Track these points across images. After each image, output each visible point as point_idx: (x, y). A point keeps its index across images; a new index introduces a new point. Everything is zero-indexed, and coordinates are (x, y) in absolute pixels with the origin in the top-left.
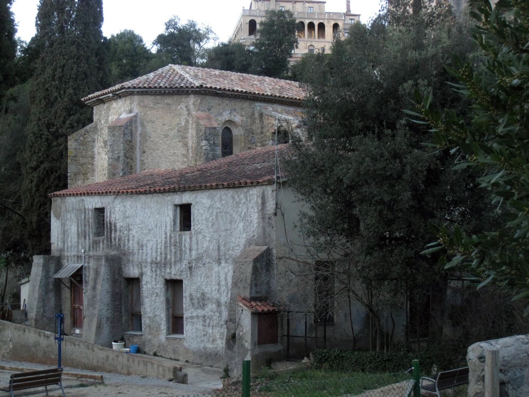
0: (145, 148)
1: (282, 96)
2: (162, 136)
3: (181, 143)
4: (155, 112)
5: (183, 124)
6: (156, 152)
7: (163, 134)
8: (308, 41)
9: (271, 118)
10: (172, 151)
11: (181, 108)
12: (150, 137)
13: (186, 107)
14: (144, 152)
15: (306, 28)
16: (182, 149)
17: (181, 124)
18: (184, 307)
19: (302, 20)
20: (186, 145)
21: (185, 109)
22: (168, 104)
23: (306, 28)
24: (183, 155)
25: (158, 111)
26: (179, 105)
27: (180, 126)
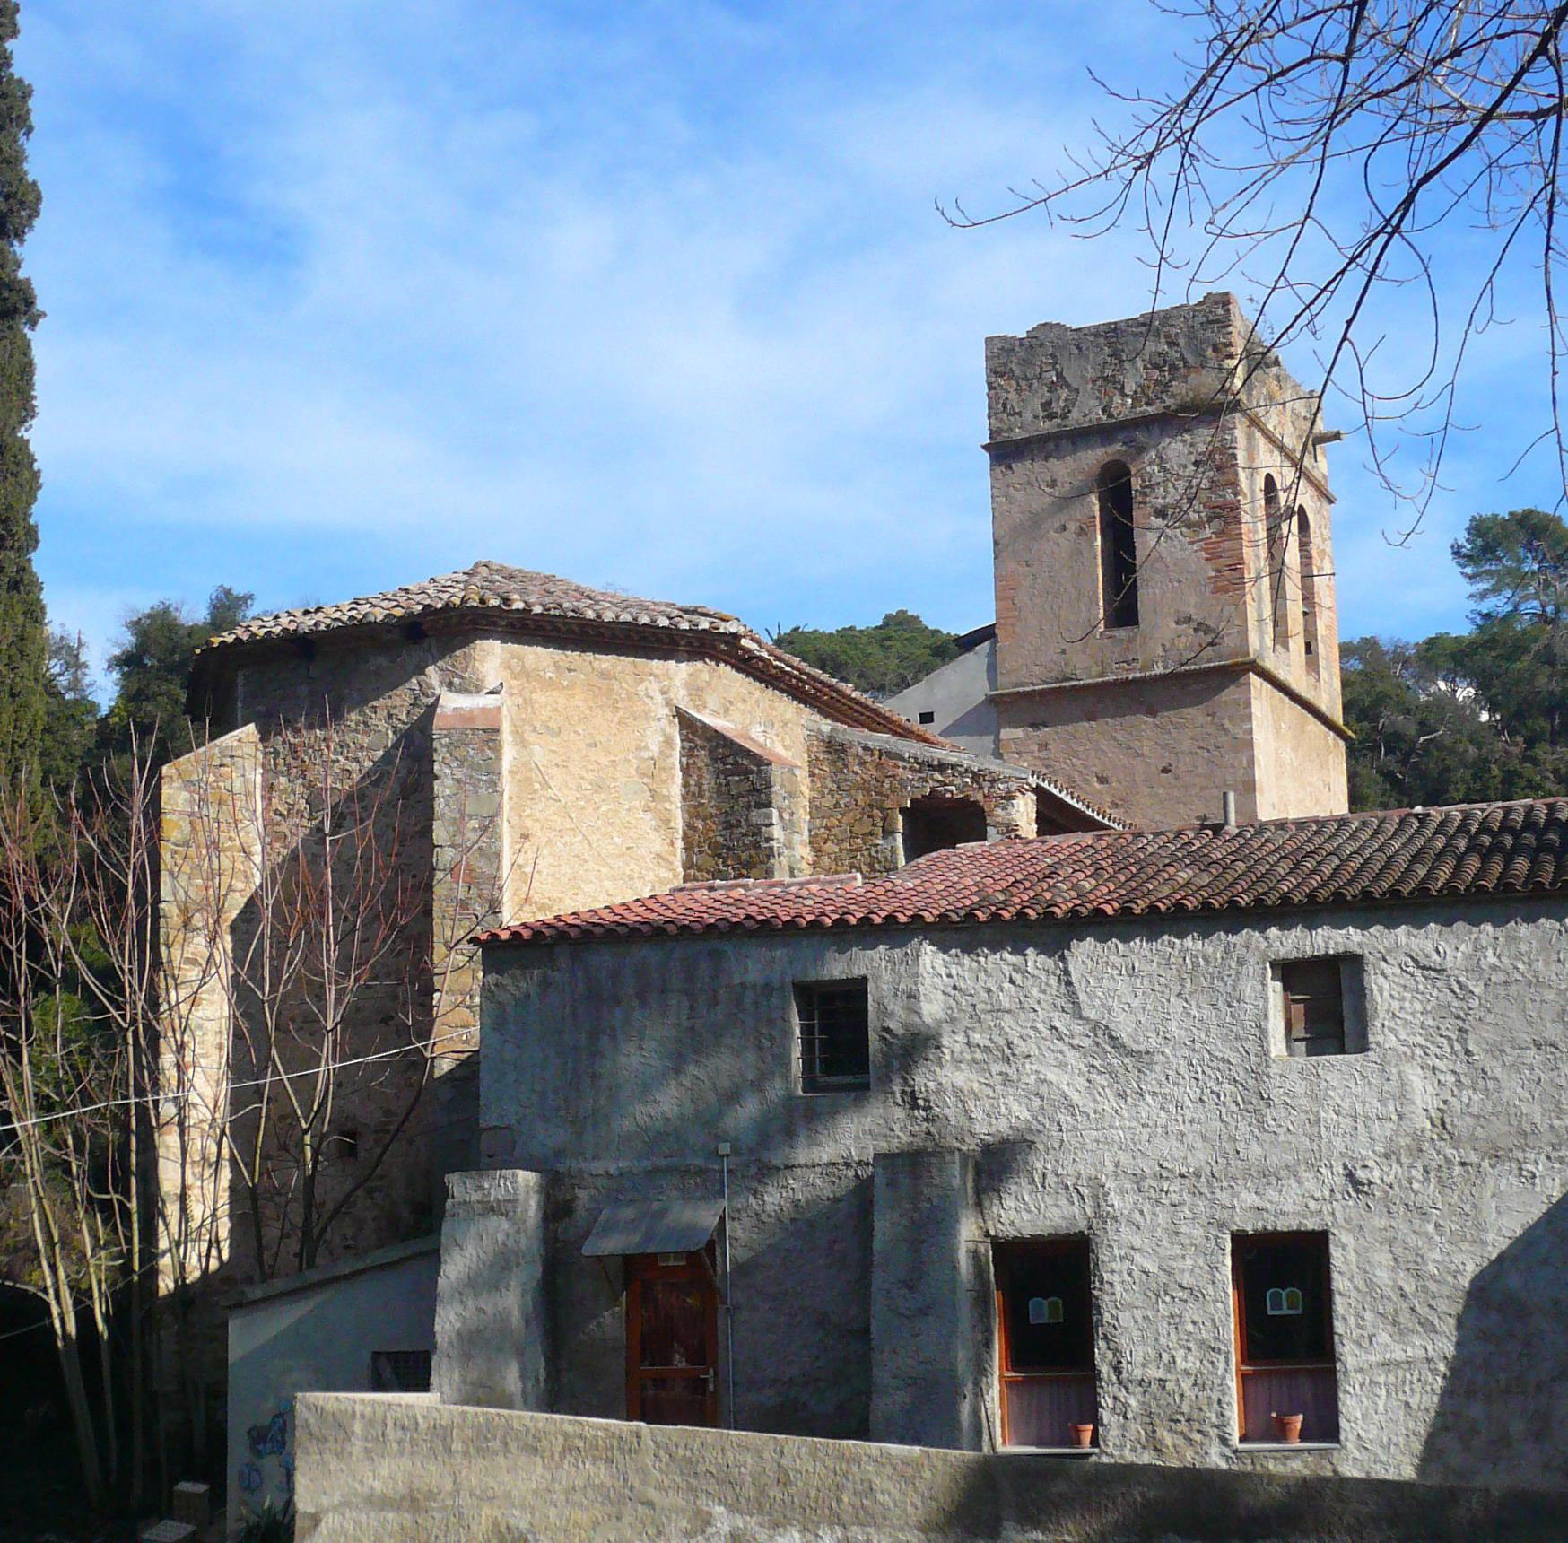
0: (529, 822)
2: (585, 785)
3: (649, 816)
4: (562, 701)
5: (655, 750)
6: (567, 839)
7: (590, 776)
9: (891, 763)
10: (618, 841)
11: (647, 695)
12: (546, 785)
13: (663, 693)
14: (525, 837)
16: (653, 835)
17: (646, 748)
18: (1339, 1326)
20: (669, 821)
21: (659, 698)
22: (604, 675)
24: (658, 856)
25: (573, 696)
26: (642, 681)
27: (645, 754)
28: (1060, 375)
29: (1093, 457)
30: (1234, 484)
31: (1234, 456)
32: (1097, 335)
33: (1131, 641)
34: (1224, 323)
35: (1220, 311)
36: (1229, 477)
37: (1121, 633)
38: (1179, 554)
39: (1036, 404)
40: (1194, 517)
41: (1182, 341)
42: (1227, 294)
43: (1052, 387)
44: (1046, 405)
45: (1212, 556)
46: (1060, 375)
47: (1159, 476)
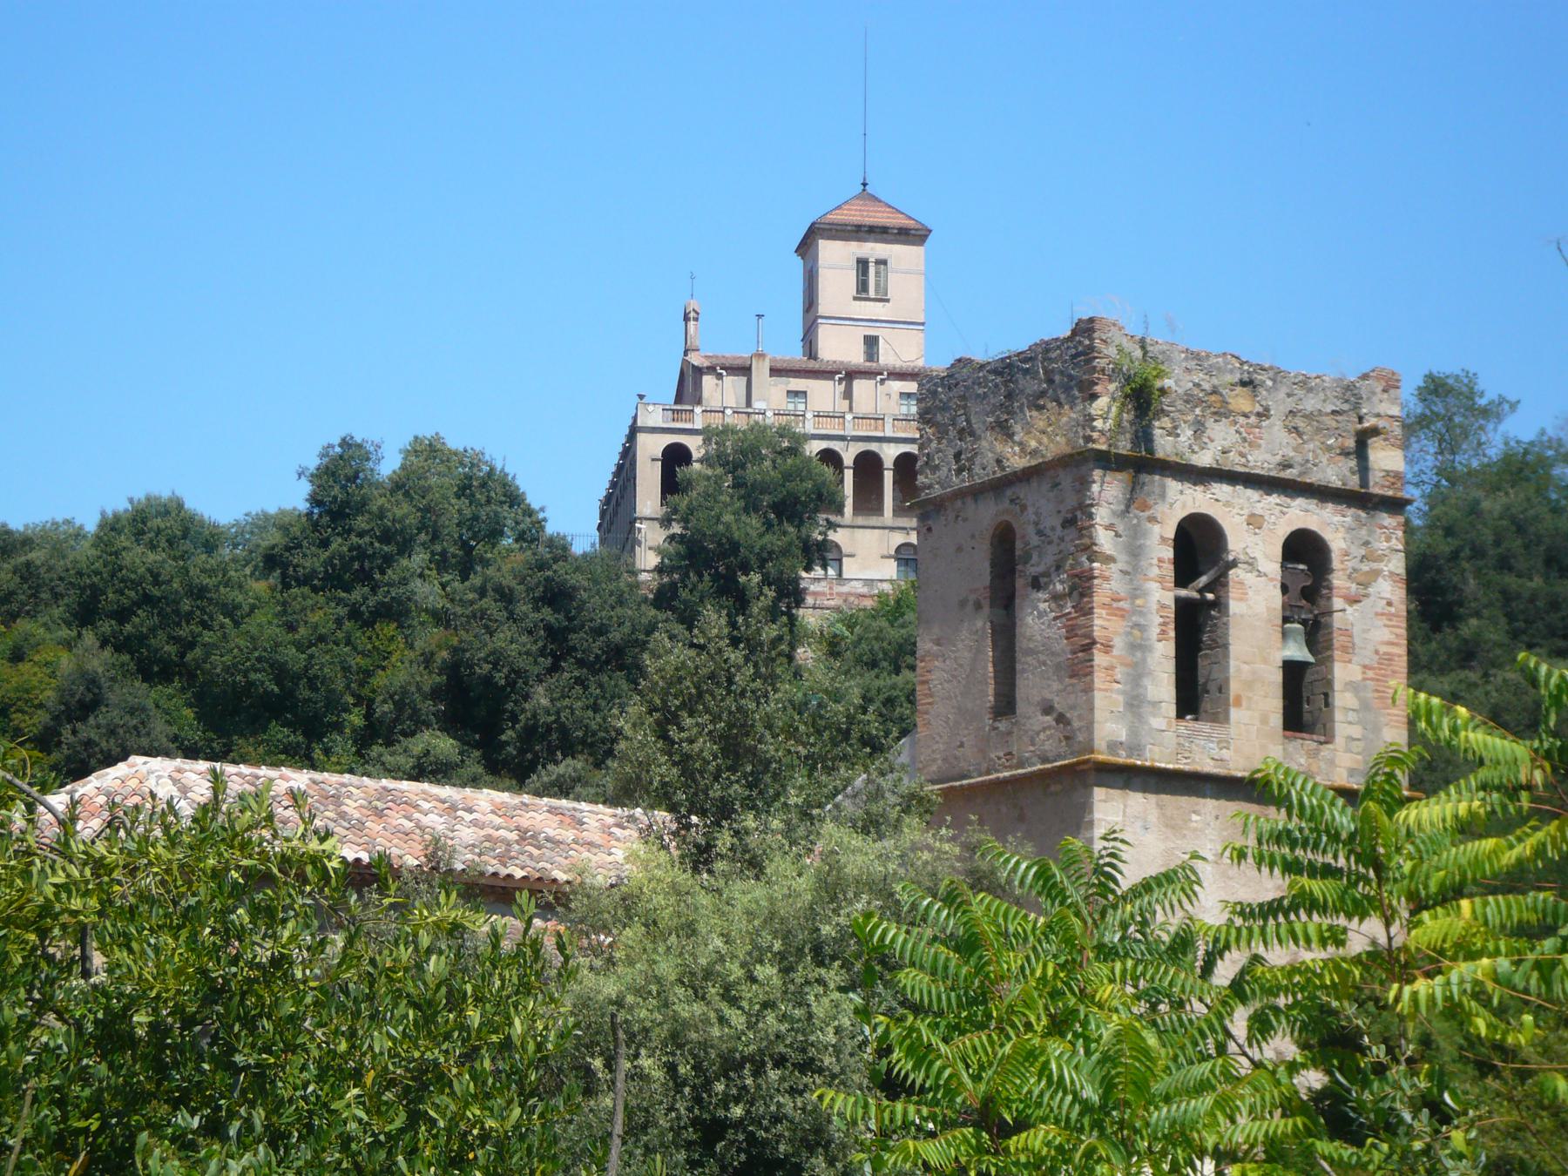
1: (504, 872)
8: (892, 529)
15: (888, 477)
19: (873, 447)
23: (888, 477)
28: (968, 421)
29: (987, 514)
30: (1090, 550)
31: (1091, 516)
32: (995, 372)
33: (1010, 733)
34: (1088, 354)
35: (1087, 342)
36: (1086, 541)
37: (1003, 725)
38: (1050, 633)
39: (951, 452)
40: (1059, 587)
41: (1057, 378)
42: (1091, 320)
43: (961, 432)
44: (957, 456)
45: (1071, 632)
46: (968, 421)
47: (1035, 540)
